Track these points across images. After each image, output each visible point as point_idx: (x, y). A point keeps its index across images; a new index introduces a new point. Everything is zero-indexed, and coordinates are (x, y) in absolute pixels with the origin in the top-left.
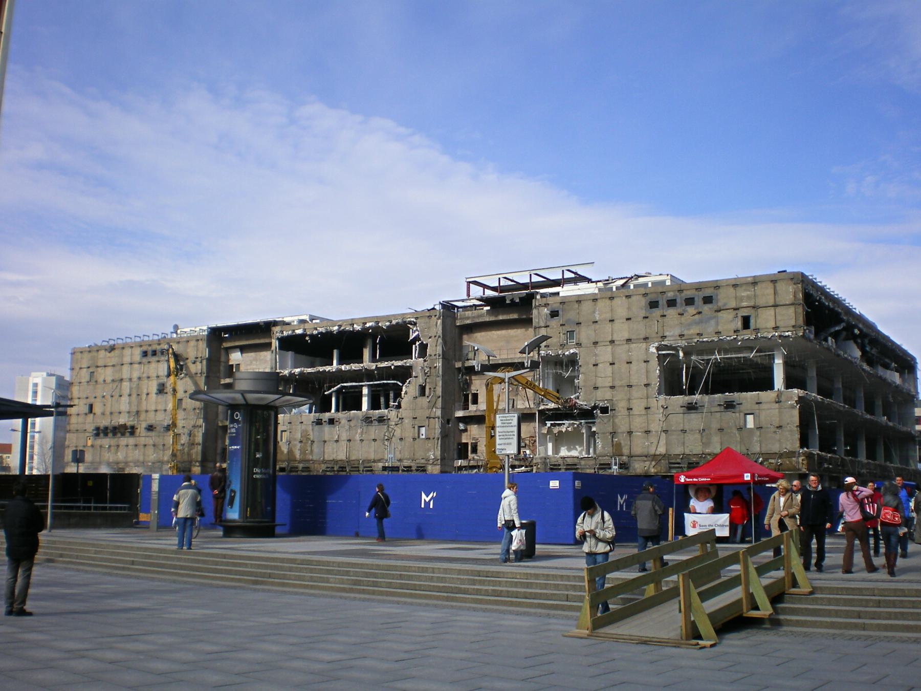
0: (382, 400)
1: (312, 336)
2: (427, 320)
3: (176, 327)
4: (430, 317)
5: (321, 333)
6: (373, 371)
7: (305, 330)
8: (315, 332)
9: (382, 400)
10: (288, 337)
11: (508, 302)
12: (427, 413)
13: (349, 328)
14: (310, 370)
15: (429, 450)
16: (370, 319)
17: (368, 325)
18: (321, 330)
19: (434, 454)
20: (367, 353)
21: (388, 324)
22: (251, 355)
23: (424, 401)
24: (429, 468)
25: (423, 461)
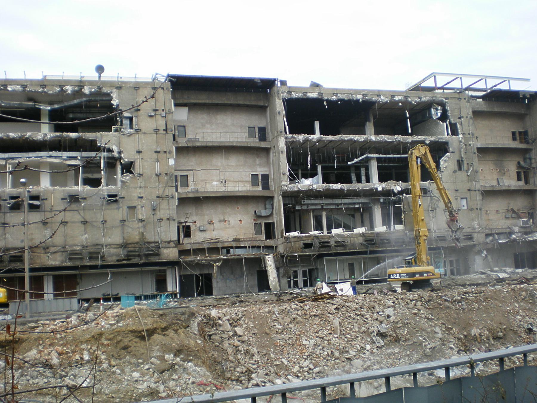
0: (353, 177)
1: (327, 101)
2: (457, 102)
3: (100, 69)
4: (459, 99)
5: (342, 100)
6: (408, 143)
7: (320, 94)
8: (334, 98)
9: (353, 177)
10: (298, 100)
11: (521, 96)
12: (468, 186)
13: (374, 99)
14: (346, 137)
15: (473, 220)
16: (399, 93)
17: (396, 98)
18: (340, 96)
19: (478, 224)
20: (370, 127)
21: (417, 100)
22: (202, 117)
23: (462, 175)
24: (475, 235)
25: (469, 230)
